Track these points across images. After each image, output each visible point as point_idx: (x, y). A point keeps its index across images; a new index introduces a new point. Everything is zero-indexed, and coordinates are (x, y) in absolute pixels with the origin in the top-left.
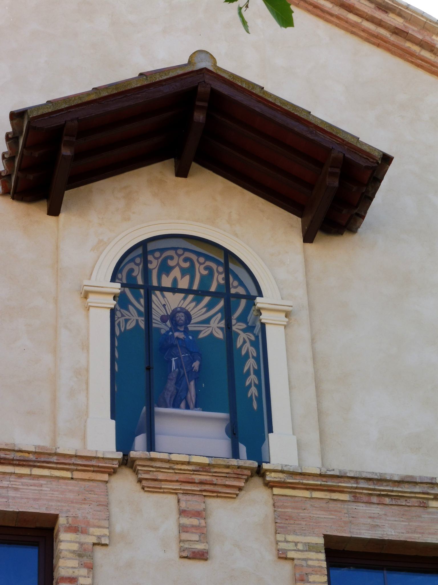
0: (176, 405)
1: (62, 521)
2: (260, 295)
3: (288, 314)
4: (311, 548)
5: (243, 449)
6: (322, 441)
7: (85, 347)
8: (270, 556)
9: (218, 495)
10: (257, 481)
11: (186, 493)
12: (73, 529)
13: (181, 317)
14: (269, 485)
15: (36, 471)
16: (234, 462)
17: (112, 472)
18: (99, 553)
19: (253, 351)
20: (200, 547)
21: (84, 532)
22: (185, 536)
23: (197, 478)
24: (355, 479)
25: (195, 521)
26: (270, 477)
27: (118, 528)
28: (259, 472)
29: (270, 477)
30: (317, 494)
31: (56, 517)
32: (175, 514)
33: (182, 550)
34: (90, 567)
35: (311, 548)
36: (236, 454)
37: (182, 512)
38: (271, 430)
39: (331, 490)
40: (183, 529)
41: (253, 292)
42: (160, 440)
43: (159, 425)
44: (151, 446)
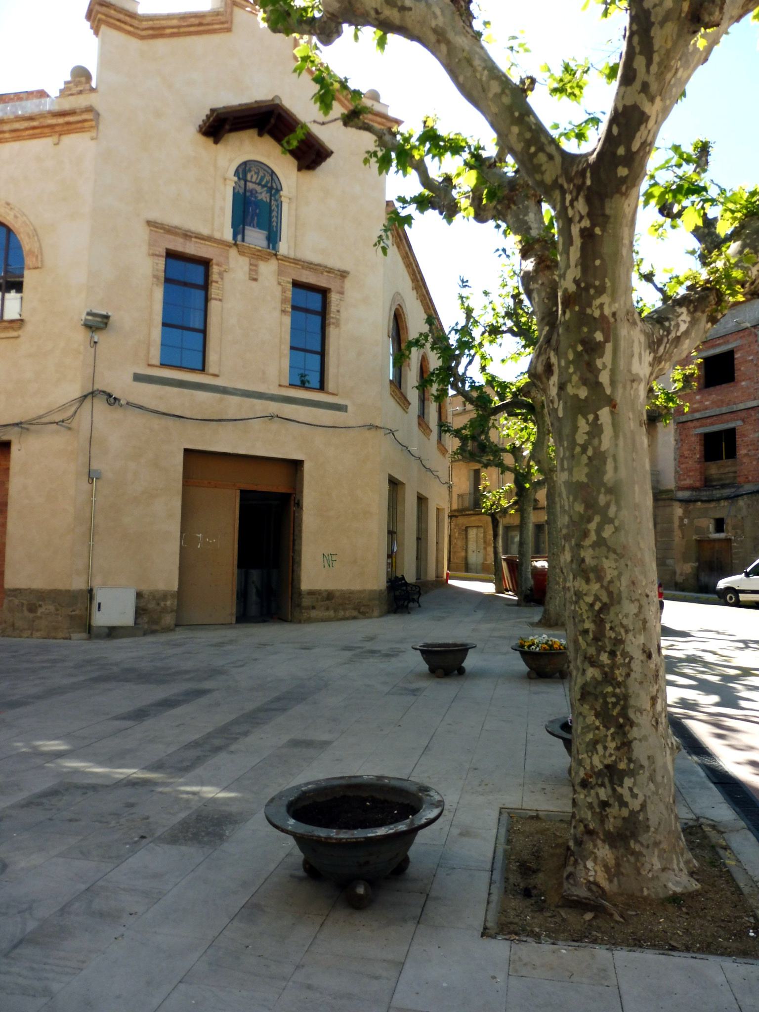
0: (250, 226)
1: (214, 261)
2: (282, 190)
3: (290, 199)
4: (288, 282)
5: (271, 245)
6: (295, 246)
7: (224, 199)
8: (276, 283)
9: (262, 260)
10: (274, 257)
11: (253, 258)
12: (218, 265)
13: (254, 192)
14: (278, 259)
15: (207, 243)
16: (268, 250)
17: (230, 247)
18: (225, 274)
19: (276, 209)
20: (255, 277)
21: (221, 266)
22: (251, 273)
23: (257, 253)
24: (304, 262)
25: (254, 268)
26: (278, 257)
27: (231, 266)
28: (276, 255)
29: (278, 257)
30: (292, 265)
31: (211, 260)
32: (248, 265)
33: (250, 277)
34: (222, 279)
35: (288, 282)
36: (269, 248)
37: (251, 264)
38: (280, 240)
39: (296, 264)
40: (250, 270)
41: (279, 188)
42: (246, 238)
43: (247, 232)
44: (243, 240)
